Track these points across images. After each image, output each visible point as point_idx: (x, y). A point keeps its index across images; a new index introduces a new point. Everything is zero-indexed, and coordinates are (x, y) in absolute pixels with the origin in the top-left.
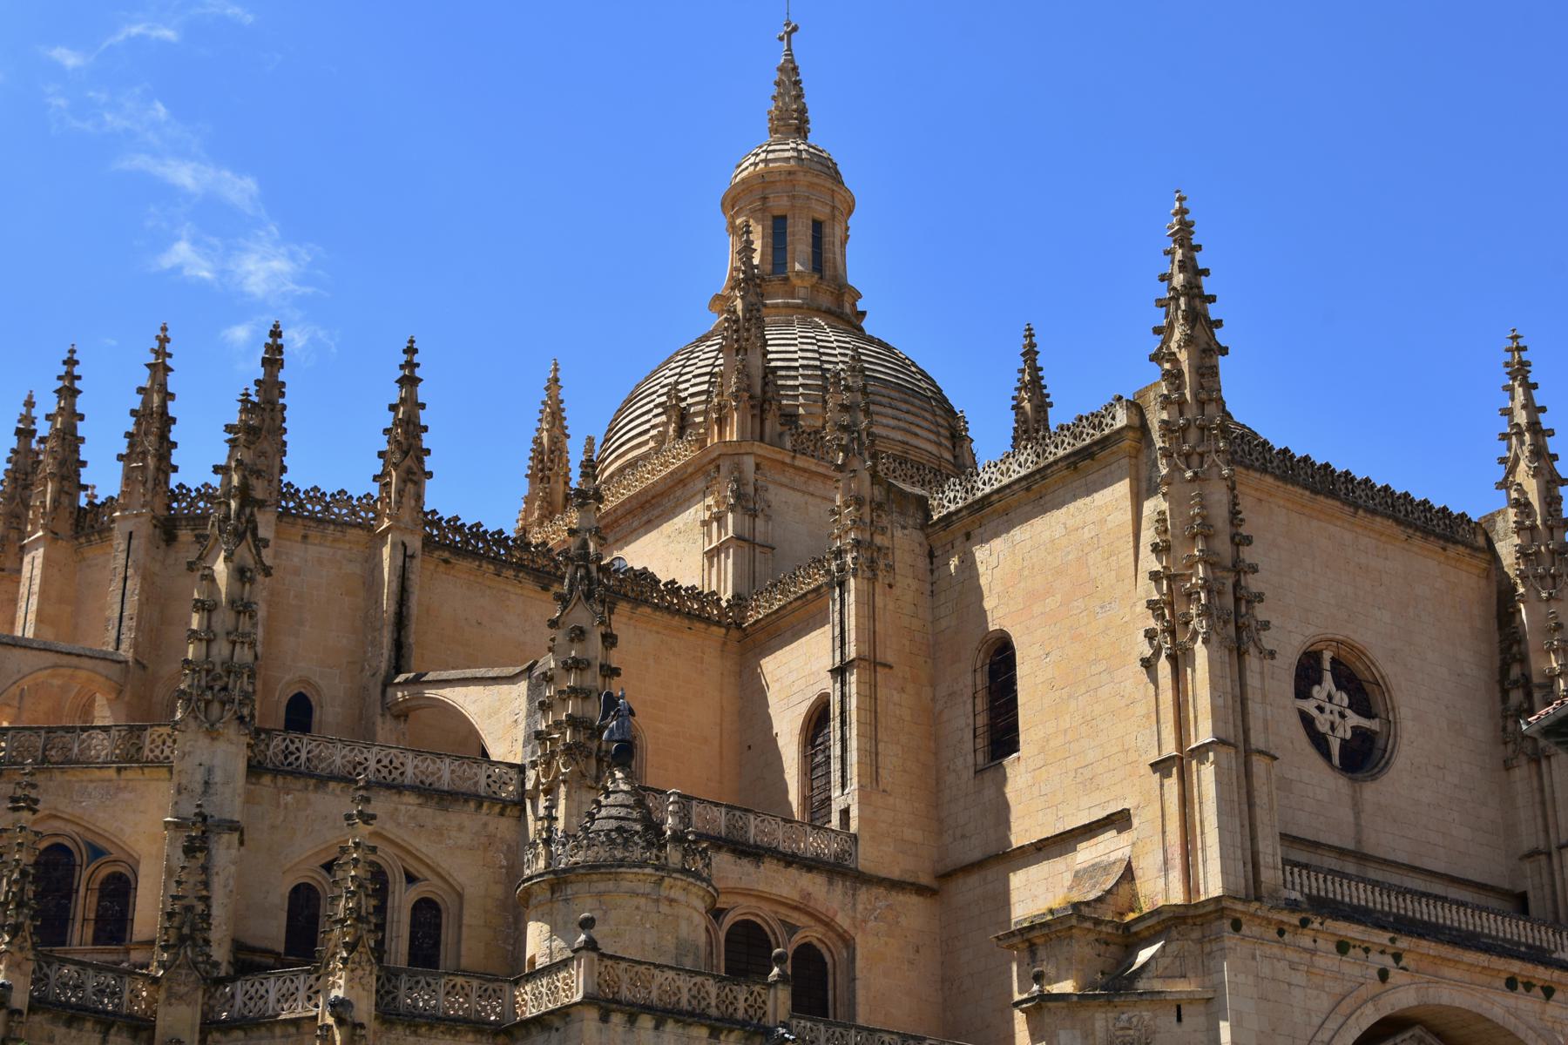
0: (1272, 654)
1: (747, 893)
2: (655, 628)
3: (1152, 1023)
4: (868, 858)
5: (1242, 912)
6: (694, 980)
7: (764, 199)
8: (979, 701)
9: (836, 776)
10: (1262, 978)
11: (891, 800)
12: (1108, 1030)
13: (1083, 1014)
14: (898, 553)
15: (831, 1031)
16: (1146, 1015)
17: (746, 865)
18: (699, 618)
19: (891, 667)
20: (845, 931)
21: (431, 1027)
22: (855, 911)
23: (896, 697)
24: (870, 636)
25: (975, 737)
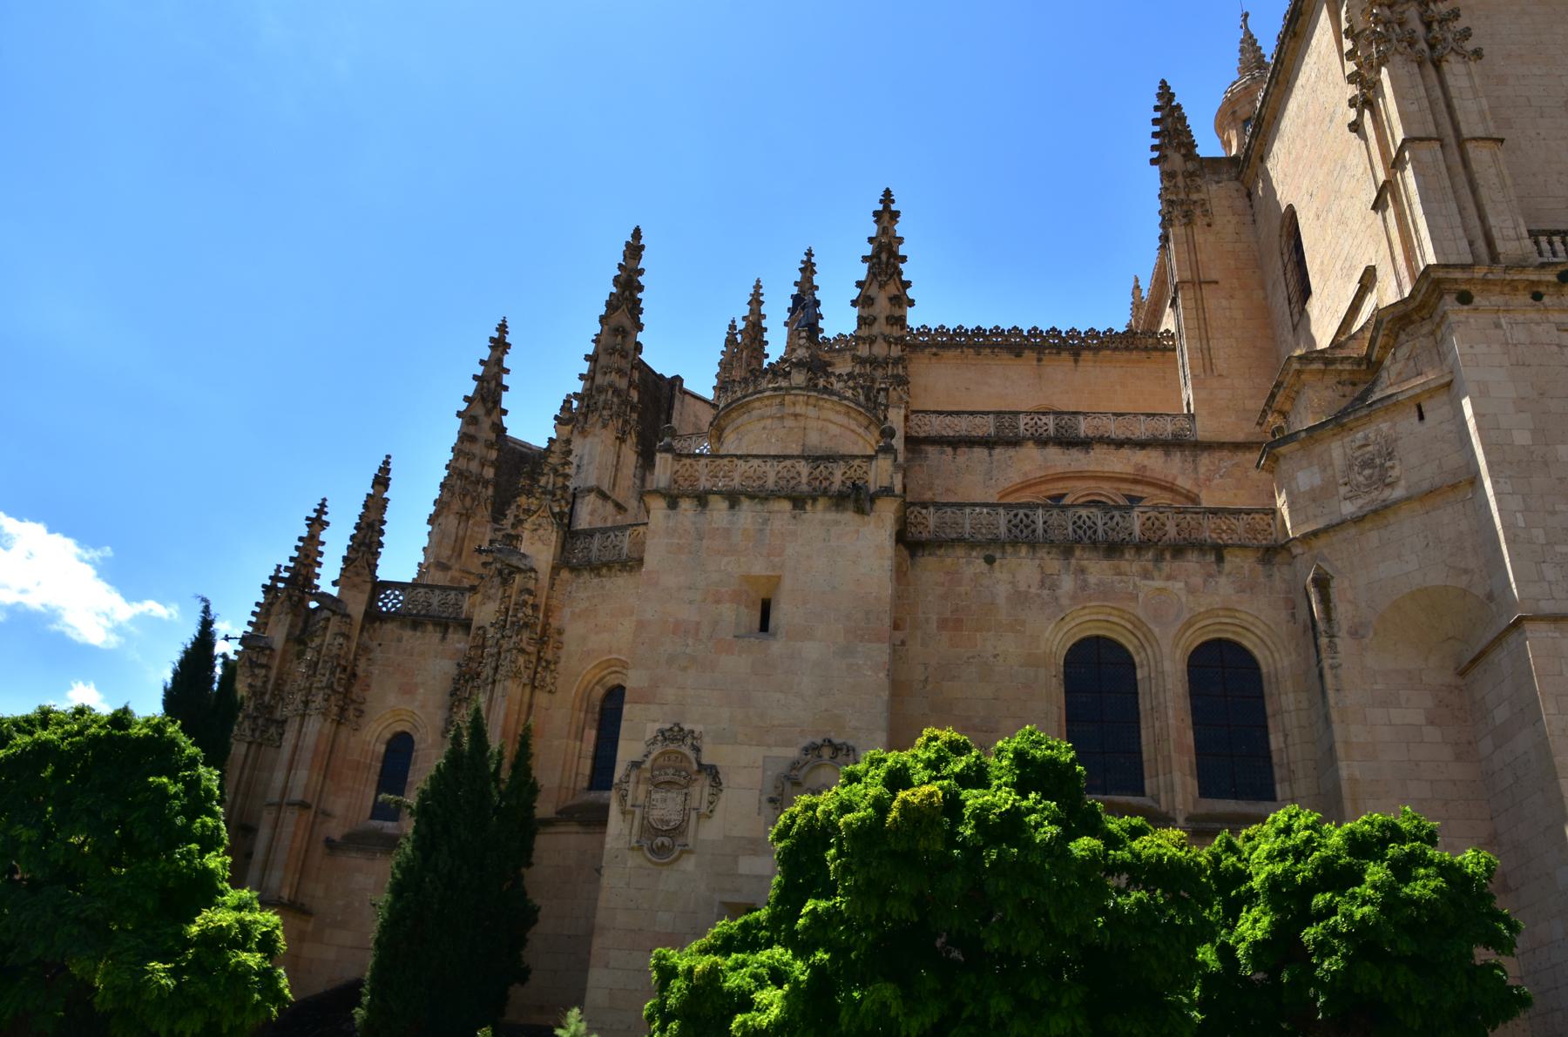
0: (1478, 54)
1: (1081, 476)
2: (1118, 365)
3: (1391, 432)
4: (1204, 429)
5: (1469, 281)
6: (783, 464)
7: (1234, 113)
8: (1289, 276)
9: (1182, 381)
10: (1515, 345)
11: (1228, 381)
12: (1345, 455)
13: (1318, 449)
14: (1215, 202)
15: (1012, 513)
16: (1385, 426)
17: (1075, 454)
18: (1155, 349)
19: (1217, 283)
20: (1189, 491)
21: (610, 569)
22: (1197, 473)
23: (1224, 303)
24: (1195, 266)
25: (1290, 303)
